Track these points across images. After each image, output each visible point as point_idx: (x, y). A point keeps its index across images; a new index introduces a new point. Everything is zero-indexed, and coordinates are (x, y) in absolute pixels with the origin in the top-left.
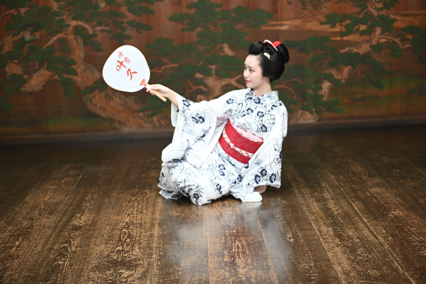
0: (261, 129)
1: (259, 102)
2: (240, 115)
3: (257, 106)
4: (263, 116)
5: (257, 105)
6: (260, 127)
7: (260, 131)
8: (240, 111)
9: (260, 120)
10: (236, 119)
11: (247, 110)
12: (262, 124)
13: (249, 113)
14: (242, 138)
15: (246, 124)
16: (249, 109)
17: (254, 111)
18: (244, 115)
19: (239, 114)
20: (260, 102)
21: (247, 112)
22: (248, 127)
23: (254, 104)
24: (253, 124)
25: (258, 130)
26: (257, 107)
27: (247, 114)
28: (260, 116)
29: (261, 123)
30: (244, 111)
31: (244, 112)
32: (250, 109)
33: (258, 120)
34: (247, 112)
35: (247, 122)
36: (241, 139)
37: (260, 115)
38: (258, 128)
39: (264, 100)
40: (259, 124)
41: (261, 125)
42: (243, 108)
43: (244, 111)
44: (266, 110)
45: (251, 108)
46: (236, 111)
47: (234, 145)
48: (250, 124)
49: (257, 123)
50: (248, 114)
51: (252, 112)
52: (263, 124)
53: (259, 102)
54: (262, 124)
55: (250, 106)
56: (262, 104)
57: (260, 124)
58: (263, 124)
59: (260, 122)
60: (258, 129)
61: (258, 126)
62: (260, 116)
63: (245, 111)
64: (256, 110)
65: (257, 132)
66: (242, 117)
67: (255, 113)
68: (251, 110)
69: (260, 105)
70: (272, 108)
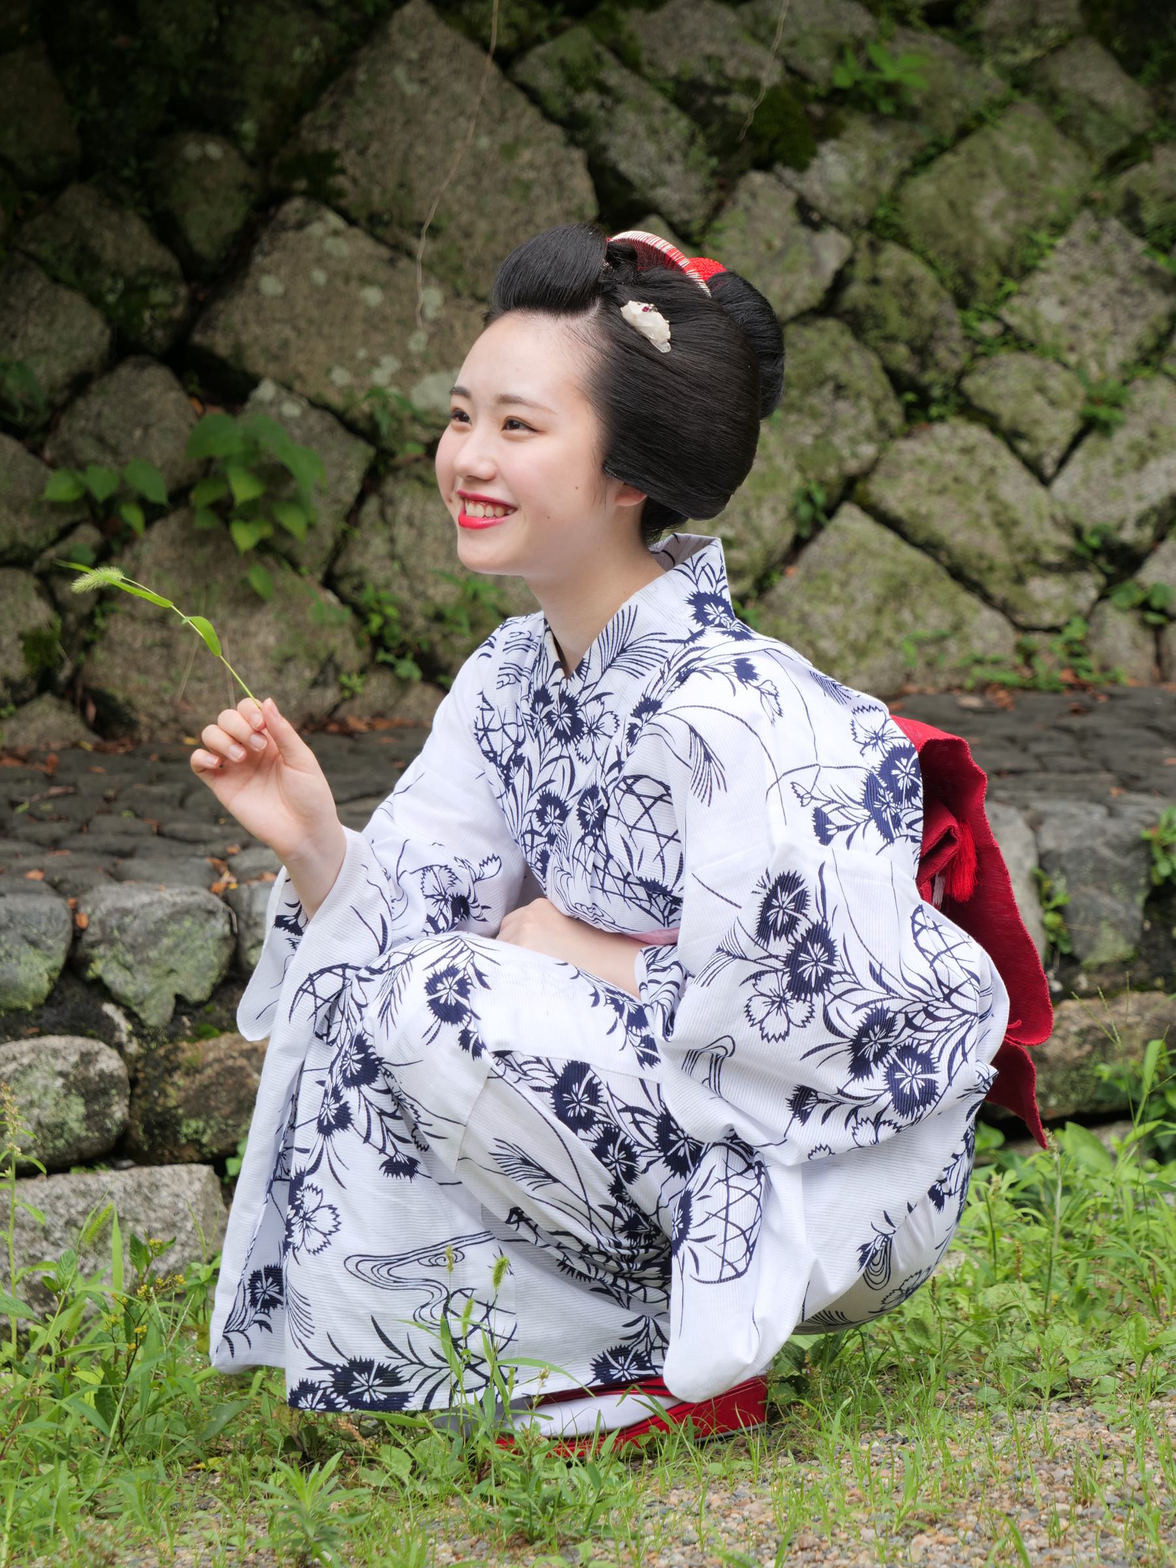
5: (571, 746)
26: (578, 764)
39: (598, 697)
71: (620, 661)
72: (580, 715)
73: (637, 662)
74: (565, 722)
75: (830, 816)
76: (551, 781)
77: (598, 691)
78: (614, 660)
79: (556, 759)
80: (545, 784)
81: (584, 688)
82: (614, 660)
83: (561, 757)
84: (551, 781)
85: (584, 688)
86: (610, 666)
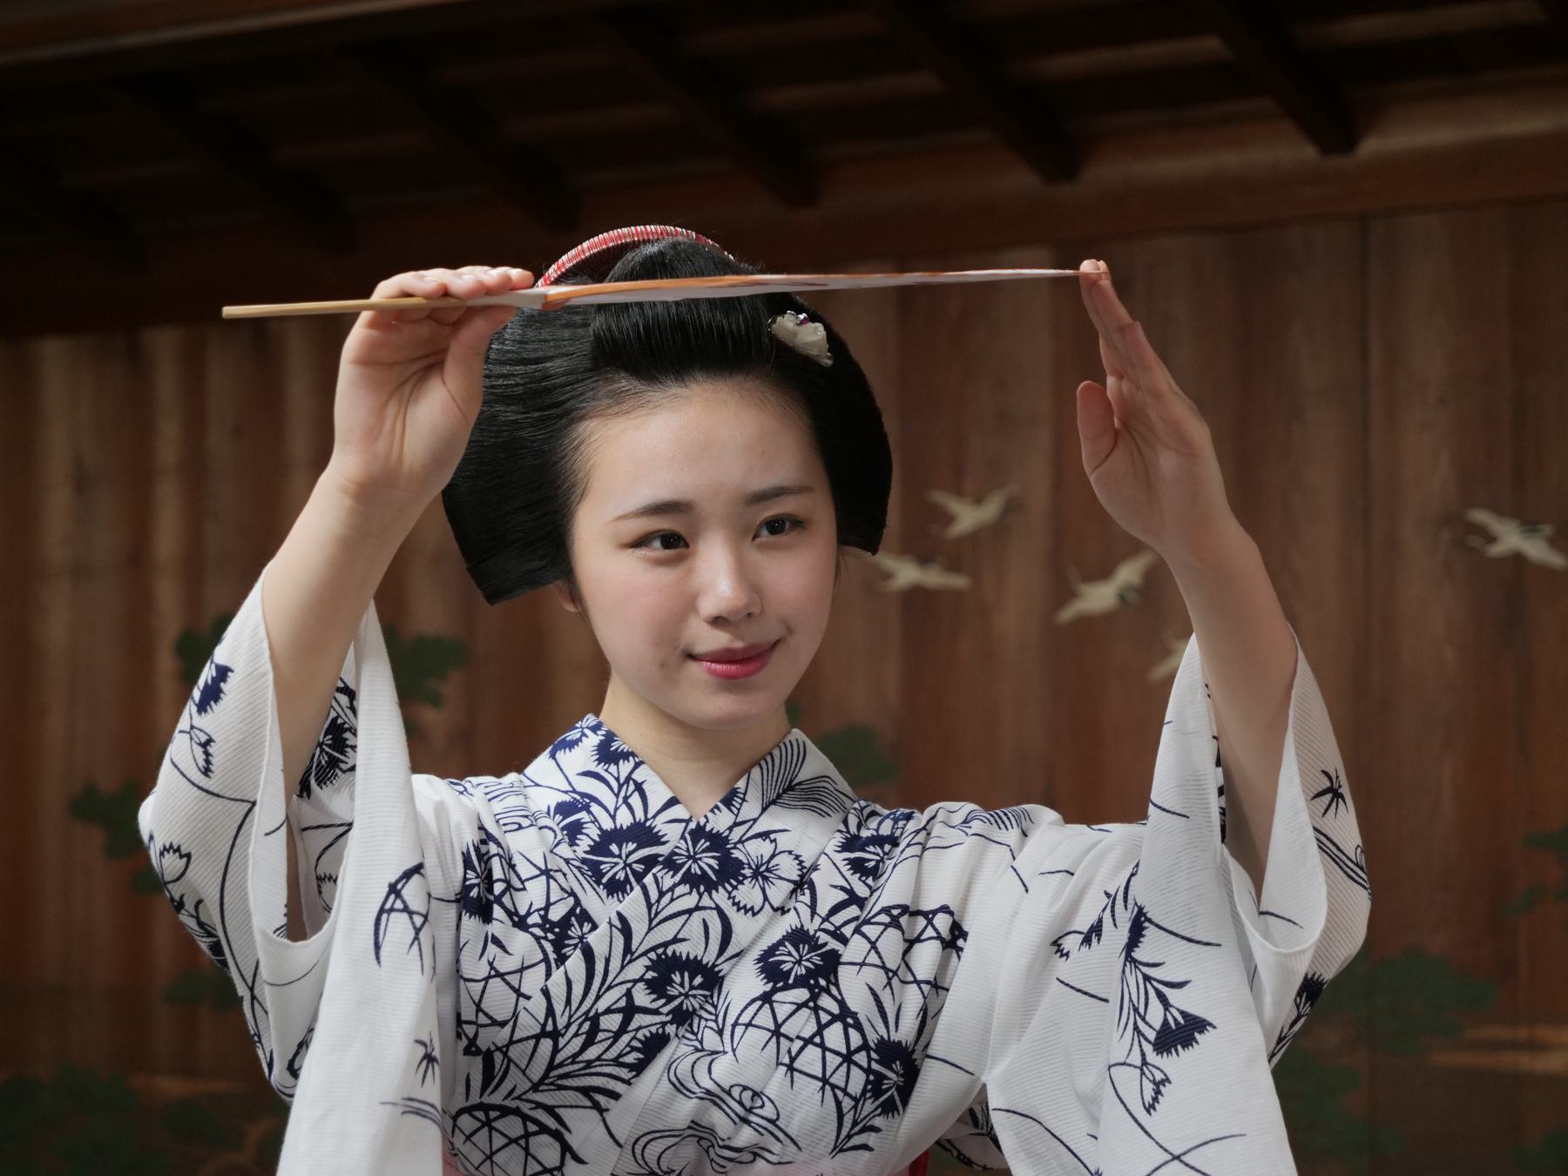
1: (730, 871)
2: (617, 1062)
3: (730, 912)
4: (832, 962)
5: (720, 897)
6: (857, 1081)
8: (595, 1020)
10: (583, 1127)
11: (658, 987)
12: (865, 1046)
16: (666, 967)
17: (725, 967)
18: (654, 1045)
19: (592, 1053)
20: (740, 864)
22: (746, 1136)
24: (776, 1085)
25: (848, 1120)
26: (738, 920)
27: (671, 1029)
28: (801, 982)
30: (630, 1010)
31: (639, 1020)
33: (803, 1024)
35: (713, 1098)
37: (801, 971)
38: (847, 1103)
39: (765, 835)
40: (833, 1061)
41: (861, 1058)
42: (606, 987)
43: (630, 1010)
45: (682, 949)
46: (555, 1035)
48: (747, 1095)
49: (811, 1059)
50: (682, 1017)
52: (872, 1038)
53: (730, 871)
55: (666, 932)
56: (757, 874)
57: (848, 1058)
58: (872, 1038)
59: (834, 1035)
61: (838, 1079)
63: (642, 997)
64: (731, 951)
66: (639, 1068)
67: (744, 983)
68: (693, 966)
69: (749, 893)
71: (786, 798)
72: (736, 854)
73: (816, 800)
74: (709, 862)
75: (1158, 1025)
76: (676, 940)
77: (758, 828)
78: (779, 796)
79: (690, 912)
80: (666, 945)
81: (736, 824)
82: (779, 796)
83: (698, 908)
84: (676, 940)
85: (736, 824)
86: (774, 802)
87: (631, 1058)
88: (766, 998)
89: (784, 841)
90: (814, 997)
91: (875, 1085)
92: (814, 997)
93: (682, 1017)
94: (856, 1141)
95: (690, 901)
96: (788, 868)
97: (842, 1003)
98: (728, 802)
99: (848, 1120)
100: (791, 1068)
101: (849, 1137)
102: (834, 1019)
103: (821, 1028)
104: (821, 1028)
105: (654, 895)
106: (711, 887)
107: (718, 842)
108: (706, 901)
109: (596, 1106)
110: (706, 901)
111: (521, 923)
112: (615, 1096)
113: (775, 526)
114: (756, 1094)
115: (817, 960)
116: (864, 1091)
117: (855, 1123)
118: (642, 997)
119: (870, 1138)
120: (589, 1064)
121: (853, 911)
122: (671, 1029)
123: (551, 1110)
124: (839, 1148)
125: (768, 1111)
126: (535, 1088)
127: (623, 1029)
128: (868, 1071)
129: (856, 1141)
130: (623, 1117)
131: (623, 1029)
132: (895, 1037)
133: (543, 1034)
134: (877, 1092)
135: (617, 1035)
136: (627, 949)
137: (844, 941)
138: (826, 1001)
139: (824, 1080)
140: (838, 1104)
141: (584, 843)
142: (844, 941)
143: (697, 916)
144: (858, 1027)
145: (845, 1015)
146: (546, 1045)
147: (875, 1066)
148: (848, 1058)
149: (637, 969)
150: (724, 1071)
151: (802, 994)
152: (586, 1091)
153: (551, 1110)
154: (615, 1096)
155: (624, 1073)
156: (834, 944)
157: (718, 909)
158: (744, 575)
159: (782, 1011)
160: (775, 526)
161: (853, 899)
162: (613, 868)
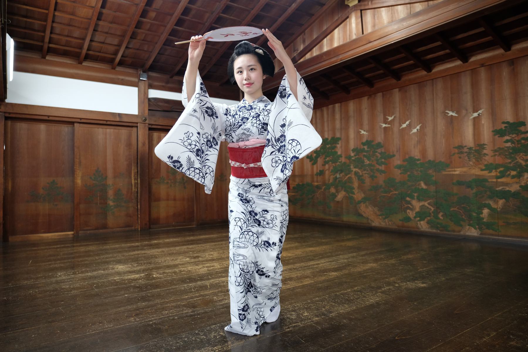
0: (262, 130)
1: (252, 108)
2: (236, 128)
4: (259, 115)
5: (250, 111)
6: (260, 127)
7: (262, 132)
9: (257, 120)
10: (233, 134)
11: (242, 120)
12: (261, 123)
13: (245, 121)
14: (249, 150)
15: (245, 132)
16: (243, 118)
17: (249, 118)
18: (241, 125)
21: (242, 122)
22: (248, 133)
23: (247, 112)
25: (260, 131)
28: (255, 117)
29: (260, 122)
30: (238, 122)
31: (239, 123)
32: (245, 118)
33: (255, 121)
34: (242, 122)
36: (248, 152)
38: (259, 129)
41: (261, 124)
43: (238, 122)
44: (260, 111)
45: (245, 117)
46: (231, 126)
47: (246, 164)
48: (248, 129)
49: (255, 125)
51: (248, 119)
52: (262, 122)
54: (261, 123)
56: (255, 109)
57: (259, 124)
58: (262, 122)
59: (258, 122)
60: (259, 131)
61: (258, 127)
62: (255, 117)
63: (240, 121)
65: (259, 134)
66: (239, 128)
68: (246, 118)
69: (253, 110)
70: (265, 106)
72: (253, 107)
74: (250, 108)
87: (238, 127)
88: (252, 120)
89: (258, 105)
90: (256, 119)
91: (263, 127)
92: (256, 119)
93: (244, 123)
94: (261, 134)
95: (247, 112)
96: (258, 108)
97: (259, 119)
98: (253, 102)
99: (260, 131)
100: (253, 126)
101: (260, 133)
102: (258, 120)
103: (257, 121)
104: (257, 121)
105: (243, 112)
106: (249, 110)
107: (251, 106)
108: (249, 112)
109: (234, 132)
110: (249, 112)
111: (230, 115)
112: (236, 131)
113: (252, 69)
114: (249, 129)
115: (258, 115)
116: (261, 128)
117: (261, 132)
118: (240, 121)
119: (263, 133)
120: (234, 128)
121: (263, 110)
122: (242, 124)
123: (230, 133)
124: (259, 134)
125: (250, 130)
126: (229, 131)
127: (237, 124)
128: (262, 126)
129: (261, 134)
130: (237, 133)
131: (237, 124)
132: (265, 122)
133: (230, 126)
134: (263, 128)
135: (237, 125)
136: (239, 117)
137: (261, 113)
138: (258, 119)
139: (256, 127)
140: (258, 129)
141: (239, 108)
142: (261, 113)
143: (247, 113)
144: (261, 121)
145: (259, 120)
146: (230, 127)
147: (262, 125)
148: (259, 124)
149: (240, 119)
150: (246, 127)
151: (255, 118)
152: (233, 131)
153: (230, 133)
154: (236, 131)
155: (237, 129)
156: (260, 114)
157: (250, 112)
158: (247, 74)
159: (253, 120)
160: (252, 69)
161: (264, 109)
162: (241, 110)
